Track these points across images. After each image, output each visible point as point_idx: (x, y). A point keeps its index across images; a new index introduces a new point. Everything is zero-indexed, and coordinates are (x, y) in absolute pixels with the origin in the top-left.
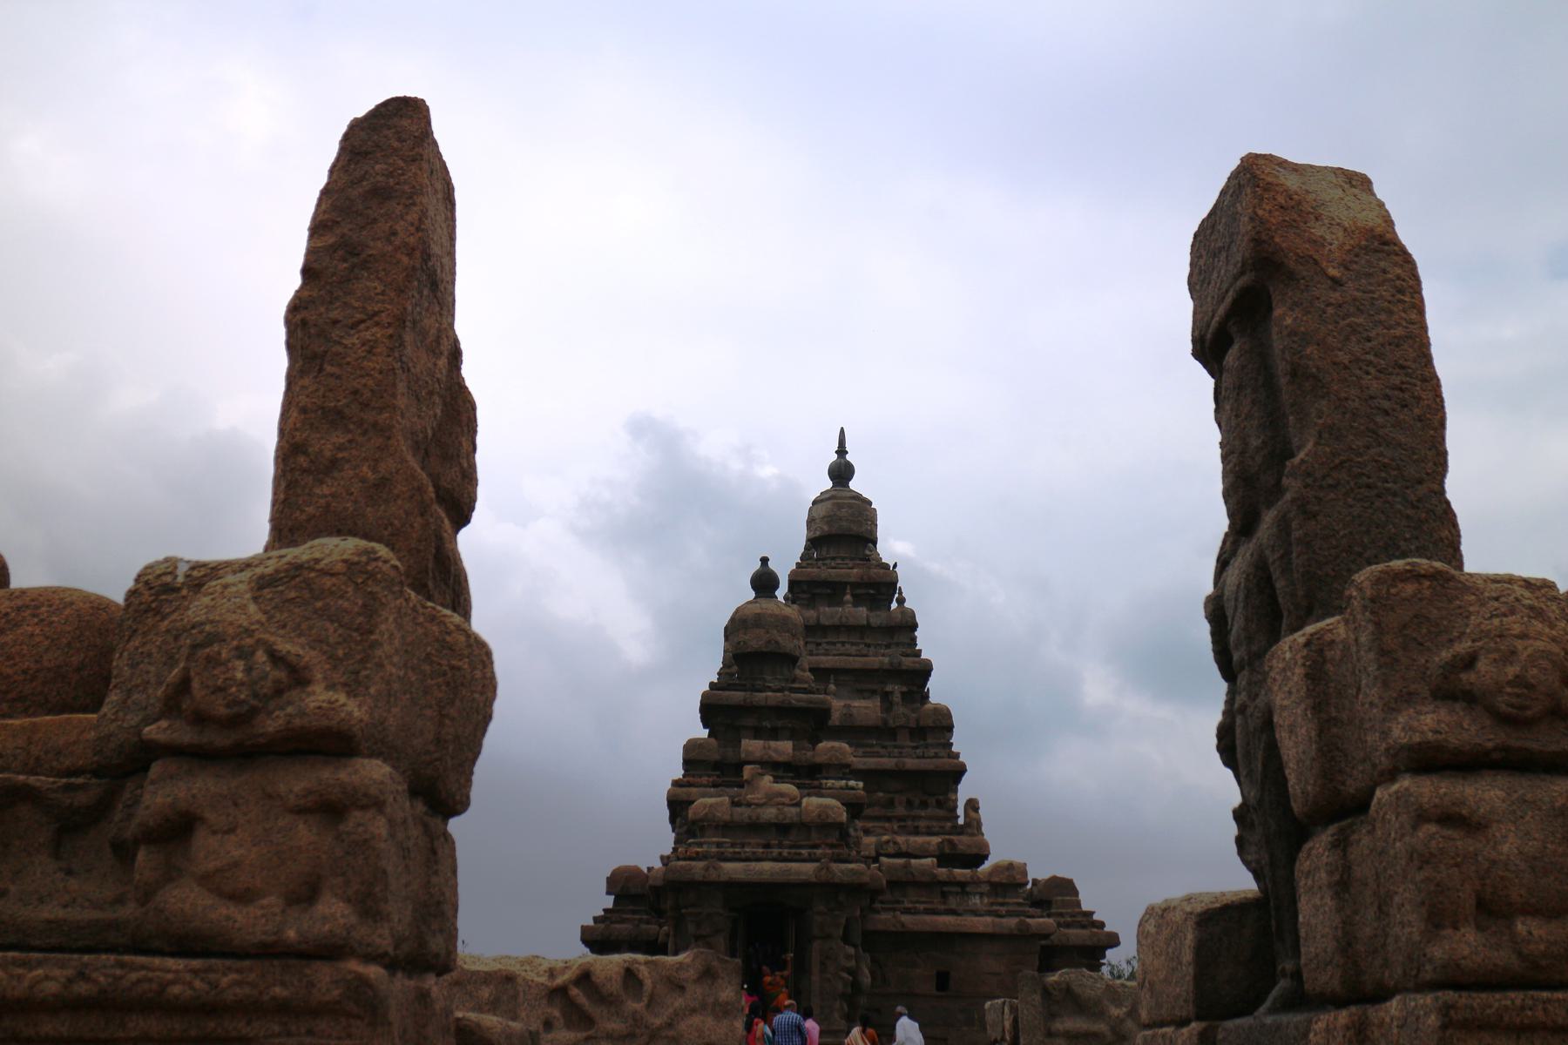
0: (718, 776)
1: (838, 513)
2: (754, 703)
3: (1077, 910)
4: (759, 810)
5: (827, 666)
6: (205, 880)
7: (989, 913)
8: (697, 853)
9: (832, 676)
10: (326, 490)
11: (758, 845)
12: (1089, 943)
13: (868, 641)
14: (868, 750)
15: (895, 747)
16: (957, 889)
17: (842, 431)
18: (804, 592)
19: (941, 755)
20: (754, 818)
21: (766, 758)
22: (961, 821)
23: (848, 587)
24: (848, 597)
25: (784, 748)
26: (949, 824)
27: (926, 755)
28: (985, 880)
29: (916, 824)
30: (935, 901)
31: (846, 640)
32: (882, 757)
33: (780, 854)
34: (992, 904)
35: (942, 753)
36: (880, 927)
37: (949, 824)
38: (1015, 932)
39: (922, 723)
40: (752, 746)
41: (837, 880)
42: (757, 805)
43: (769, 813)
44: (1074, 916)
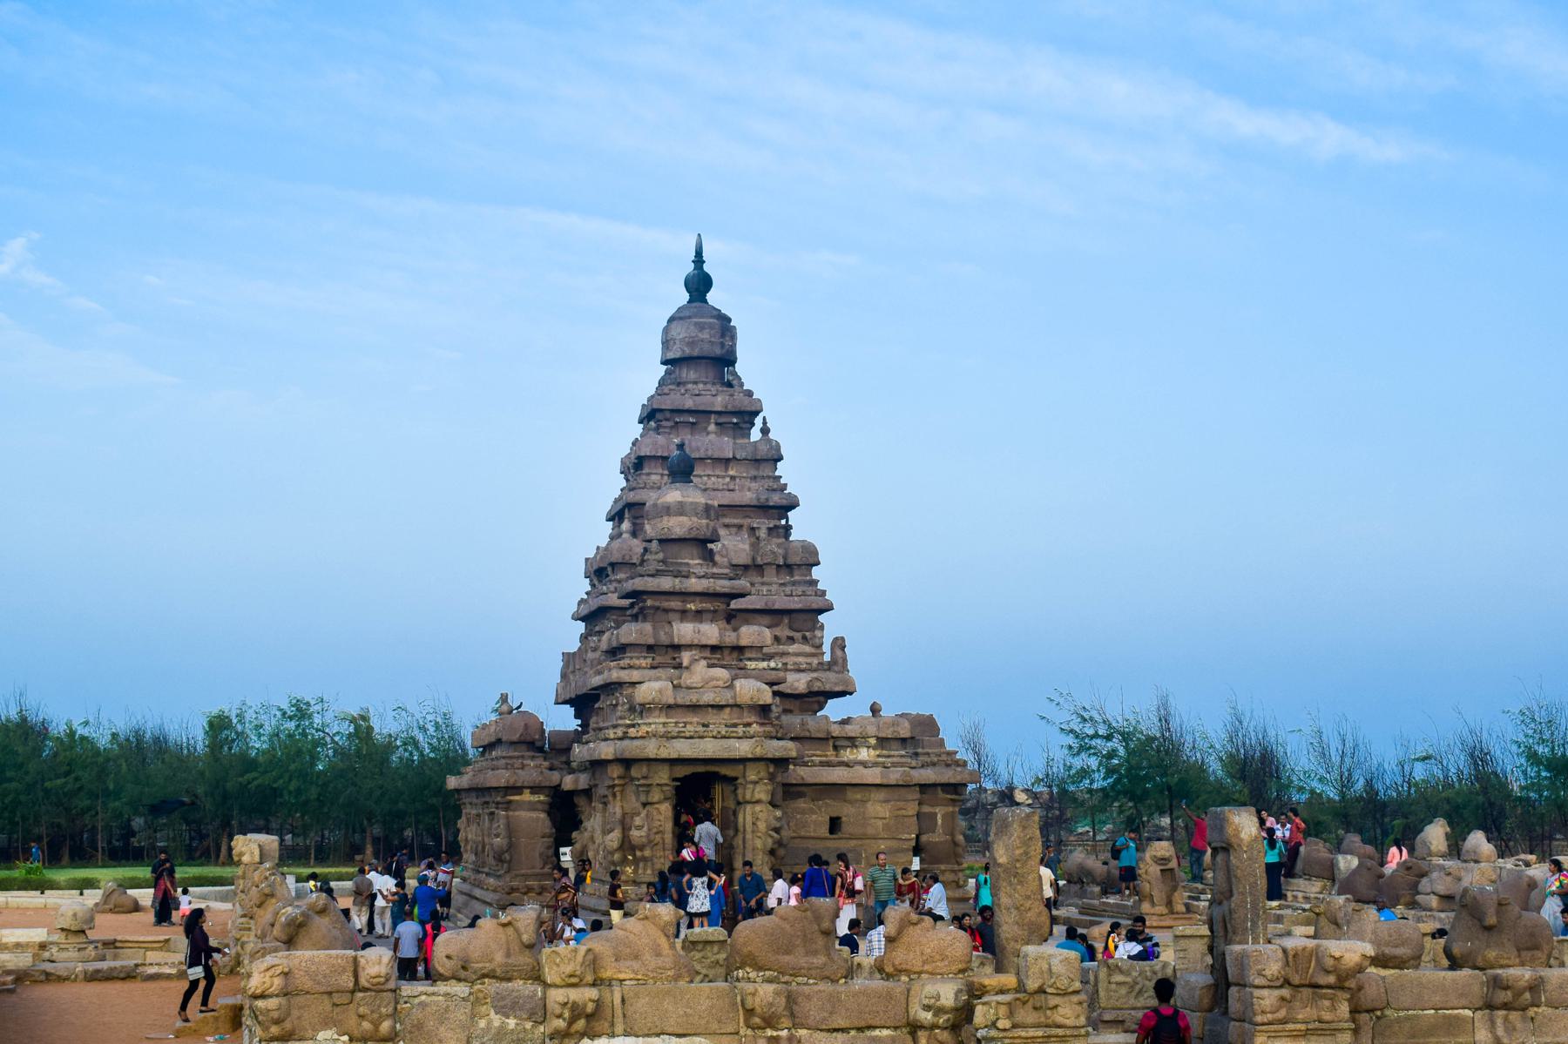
1: (700, 335)
2: (683, 590)
3: (942, 750)
6: (1061, 1016)
7: (876, 764)
8: (647, 732)
10: (1029, 915)
12: (953, 781)
13: (731, 473)
15: (763, 584)
17: (699, 235)
18: (667, 420)
19: (809, 593)
21: (696, 642)
22: (827, 658)
25: (711, 632)
26: (815, 661)
31: (710, 473)
34: (879, 756)
35: (809, 590)
37: (815, 661)
38: (901, 783)
39: (790, 561)
40: (685, 631)
43: (708, 697)
44: (940, 756)
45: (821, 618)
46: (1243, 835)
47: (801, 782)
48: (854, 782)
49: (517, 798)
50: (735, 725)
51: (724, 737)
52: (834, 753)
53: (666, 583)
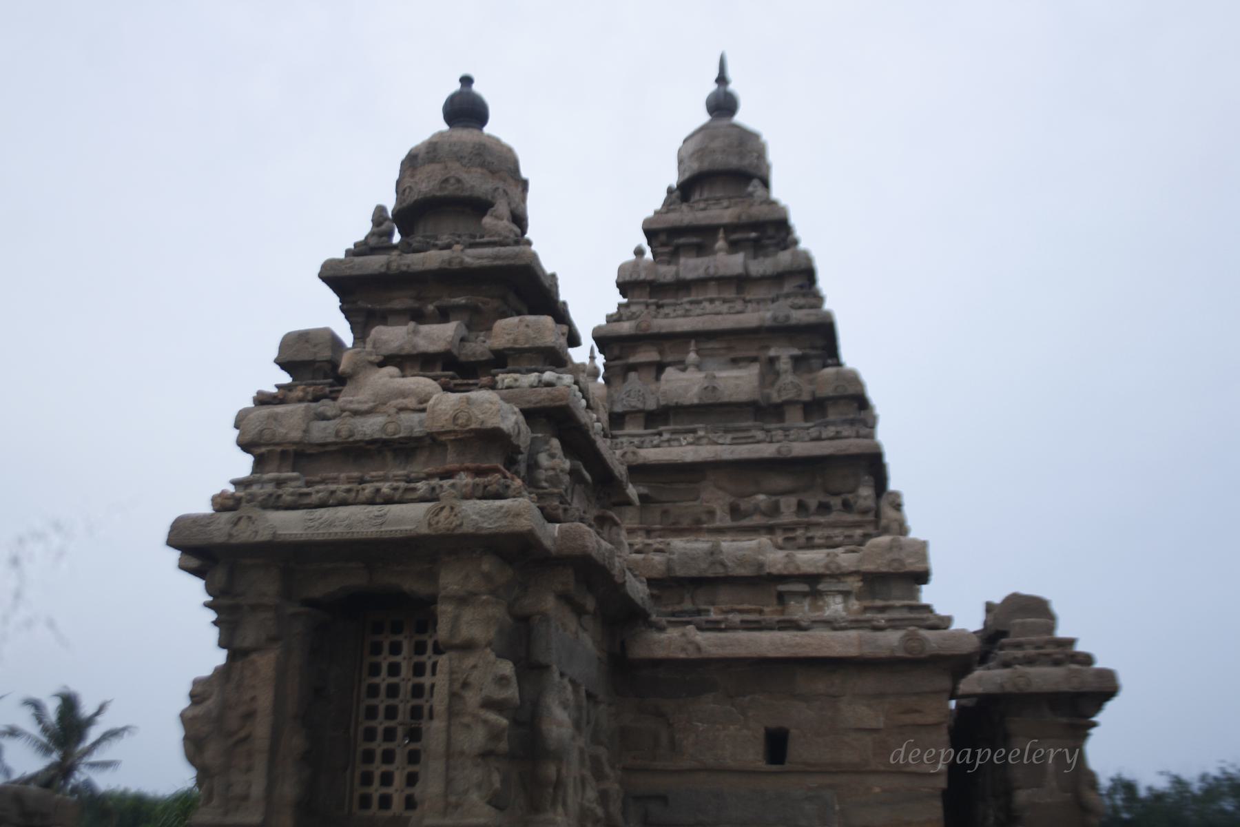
0: (331, 385)
2: (404, 268)
7: (856, 624)
9: (693, 343)
11: (350, 480)
12: (1065, 688)
13: (748, 297)
18: (663, 245)
19: (845, 433)
20: (344, 433)
21: (408, 349)
23: (721, 231)
24: (720, 244)
27: (824, 436)
28: (853, 569)
29: (810, 534)
30: (766, 609)
32: (758, 442)
34: (866, 609)
35: (846, 430)
36: (660, 653)
38: (900, 654)
41: (467, 528)
42: (356, 413)
43: (370, 427)
47: (694, 655)
51: (389, 501)
52: (779, 608)
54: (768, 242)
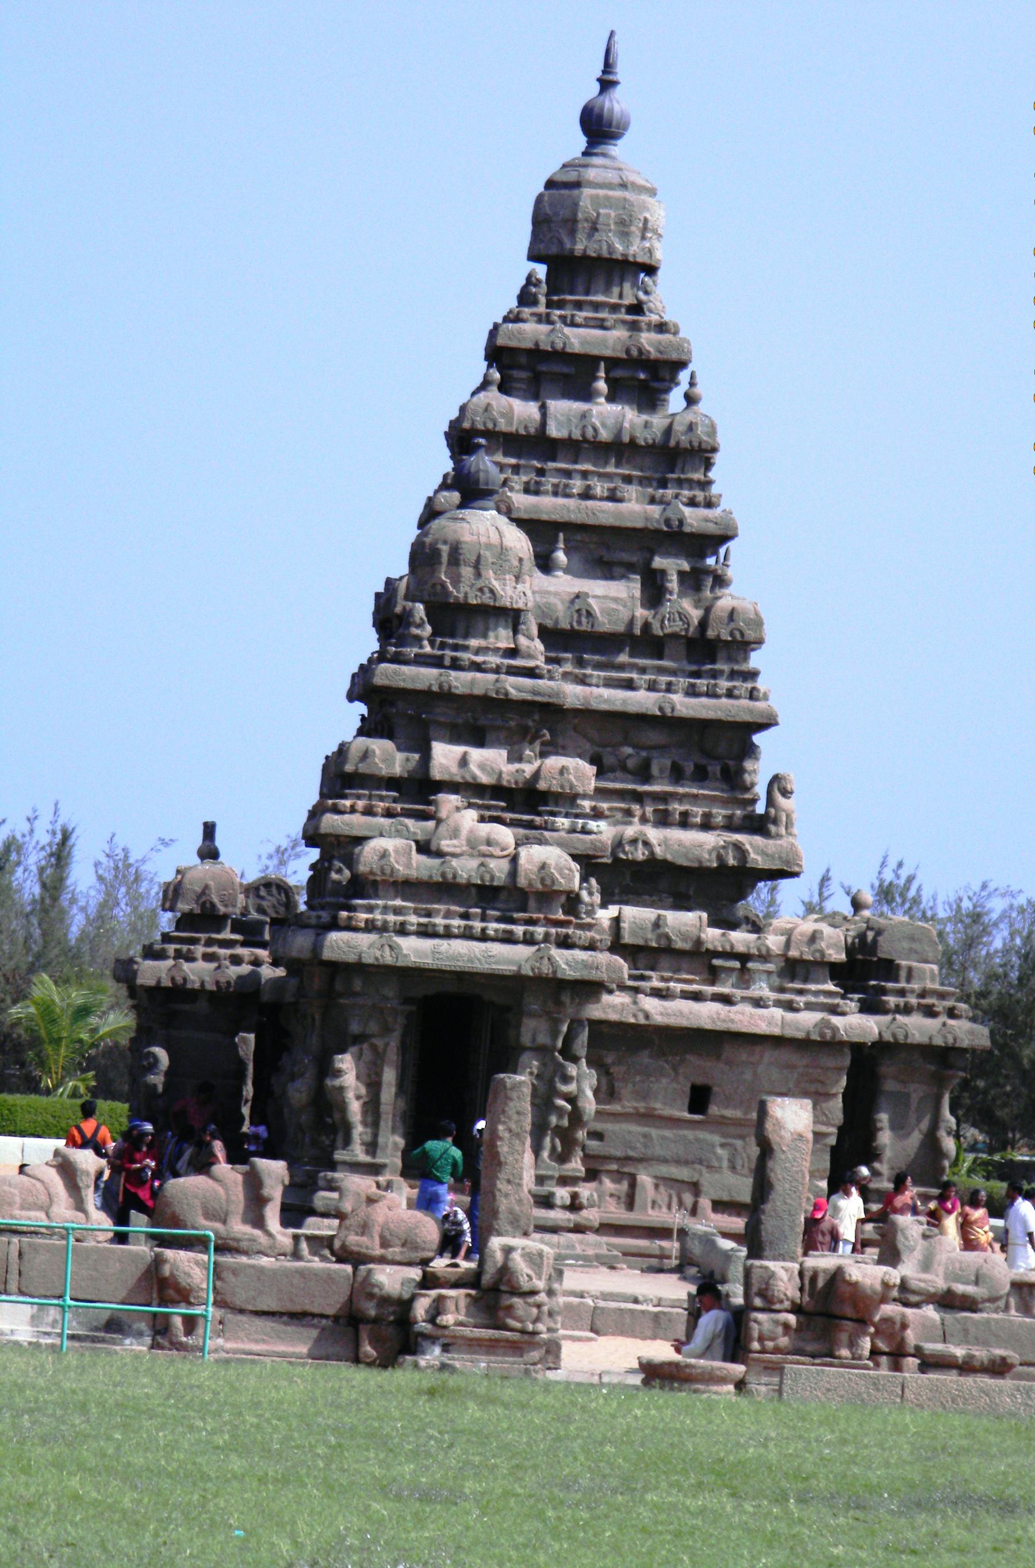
2: (454, 690)
4: (455, 863)
5: (555, 517)
7: (778, 1003)
8: (367, 921)
9: (561, 536)
14: (614, 674)
15: (661, 670)
16: (737, 964)
17: (612, 34)
23: (602, 364)
33: (484, 930)
38: (815, 1037)
39: (711, 633)
42: (454, 855)
45: (757, 739)
46: (783, 1133)
47: (642, 1021)
48: (734, 1027)
49: (186, 1007)
50: (512, 921)
52: (711, 977)
53: (425, 677)
54: (655, 385)
